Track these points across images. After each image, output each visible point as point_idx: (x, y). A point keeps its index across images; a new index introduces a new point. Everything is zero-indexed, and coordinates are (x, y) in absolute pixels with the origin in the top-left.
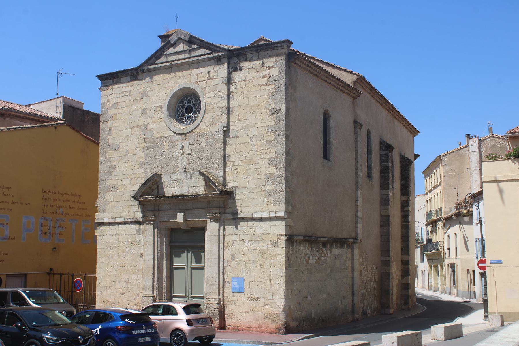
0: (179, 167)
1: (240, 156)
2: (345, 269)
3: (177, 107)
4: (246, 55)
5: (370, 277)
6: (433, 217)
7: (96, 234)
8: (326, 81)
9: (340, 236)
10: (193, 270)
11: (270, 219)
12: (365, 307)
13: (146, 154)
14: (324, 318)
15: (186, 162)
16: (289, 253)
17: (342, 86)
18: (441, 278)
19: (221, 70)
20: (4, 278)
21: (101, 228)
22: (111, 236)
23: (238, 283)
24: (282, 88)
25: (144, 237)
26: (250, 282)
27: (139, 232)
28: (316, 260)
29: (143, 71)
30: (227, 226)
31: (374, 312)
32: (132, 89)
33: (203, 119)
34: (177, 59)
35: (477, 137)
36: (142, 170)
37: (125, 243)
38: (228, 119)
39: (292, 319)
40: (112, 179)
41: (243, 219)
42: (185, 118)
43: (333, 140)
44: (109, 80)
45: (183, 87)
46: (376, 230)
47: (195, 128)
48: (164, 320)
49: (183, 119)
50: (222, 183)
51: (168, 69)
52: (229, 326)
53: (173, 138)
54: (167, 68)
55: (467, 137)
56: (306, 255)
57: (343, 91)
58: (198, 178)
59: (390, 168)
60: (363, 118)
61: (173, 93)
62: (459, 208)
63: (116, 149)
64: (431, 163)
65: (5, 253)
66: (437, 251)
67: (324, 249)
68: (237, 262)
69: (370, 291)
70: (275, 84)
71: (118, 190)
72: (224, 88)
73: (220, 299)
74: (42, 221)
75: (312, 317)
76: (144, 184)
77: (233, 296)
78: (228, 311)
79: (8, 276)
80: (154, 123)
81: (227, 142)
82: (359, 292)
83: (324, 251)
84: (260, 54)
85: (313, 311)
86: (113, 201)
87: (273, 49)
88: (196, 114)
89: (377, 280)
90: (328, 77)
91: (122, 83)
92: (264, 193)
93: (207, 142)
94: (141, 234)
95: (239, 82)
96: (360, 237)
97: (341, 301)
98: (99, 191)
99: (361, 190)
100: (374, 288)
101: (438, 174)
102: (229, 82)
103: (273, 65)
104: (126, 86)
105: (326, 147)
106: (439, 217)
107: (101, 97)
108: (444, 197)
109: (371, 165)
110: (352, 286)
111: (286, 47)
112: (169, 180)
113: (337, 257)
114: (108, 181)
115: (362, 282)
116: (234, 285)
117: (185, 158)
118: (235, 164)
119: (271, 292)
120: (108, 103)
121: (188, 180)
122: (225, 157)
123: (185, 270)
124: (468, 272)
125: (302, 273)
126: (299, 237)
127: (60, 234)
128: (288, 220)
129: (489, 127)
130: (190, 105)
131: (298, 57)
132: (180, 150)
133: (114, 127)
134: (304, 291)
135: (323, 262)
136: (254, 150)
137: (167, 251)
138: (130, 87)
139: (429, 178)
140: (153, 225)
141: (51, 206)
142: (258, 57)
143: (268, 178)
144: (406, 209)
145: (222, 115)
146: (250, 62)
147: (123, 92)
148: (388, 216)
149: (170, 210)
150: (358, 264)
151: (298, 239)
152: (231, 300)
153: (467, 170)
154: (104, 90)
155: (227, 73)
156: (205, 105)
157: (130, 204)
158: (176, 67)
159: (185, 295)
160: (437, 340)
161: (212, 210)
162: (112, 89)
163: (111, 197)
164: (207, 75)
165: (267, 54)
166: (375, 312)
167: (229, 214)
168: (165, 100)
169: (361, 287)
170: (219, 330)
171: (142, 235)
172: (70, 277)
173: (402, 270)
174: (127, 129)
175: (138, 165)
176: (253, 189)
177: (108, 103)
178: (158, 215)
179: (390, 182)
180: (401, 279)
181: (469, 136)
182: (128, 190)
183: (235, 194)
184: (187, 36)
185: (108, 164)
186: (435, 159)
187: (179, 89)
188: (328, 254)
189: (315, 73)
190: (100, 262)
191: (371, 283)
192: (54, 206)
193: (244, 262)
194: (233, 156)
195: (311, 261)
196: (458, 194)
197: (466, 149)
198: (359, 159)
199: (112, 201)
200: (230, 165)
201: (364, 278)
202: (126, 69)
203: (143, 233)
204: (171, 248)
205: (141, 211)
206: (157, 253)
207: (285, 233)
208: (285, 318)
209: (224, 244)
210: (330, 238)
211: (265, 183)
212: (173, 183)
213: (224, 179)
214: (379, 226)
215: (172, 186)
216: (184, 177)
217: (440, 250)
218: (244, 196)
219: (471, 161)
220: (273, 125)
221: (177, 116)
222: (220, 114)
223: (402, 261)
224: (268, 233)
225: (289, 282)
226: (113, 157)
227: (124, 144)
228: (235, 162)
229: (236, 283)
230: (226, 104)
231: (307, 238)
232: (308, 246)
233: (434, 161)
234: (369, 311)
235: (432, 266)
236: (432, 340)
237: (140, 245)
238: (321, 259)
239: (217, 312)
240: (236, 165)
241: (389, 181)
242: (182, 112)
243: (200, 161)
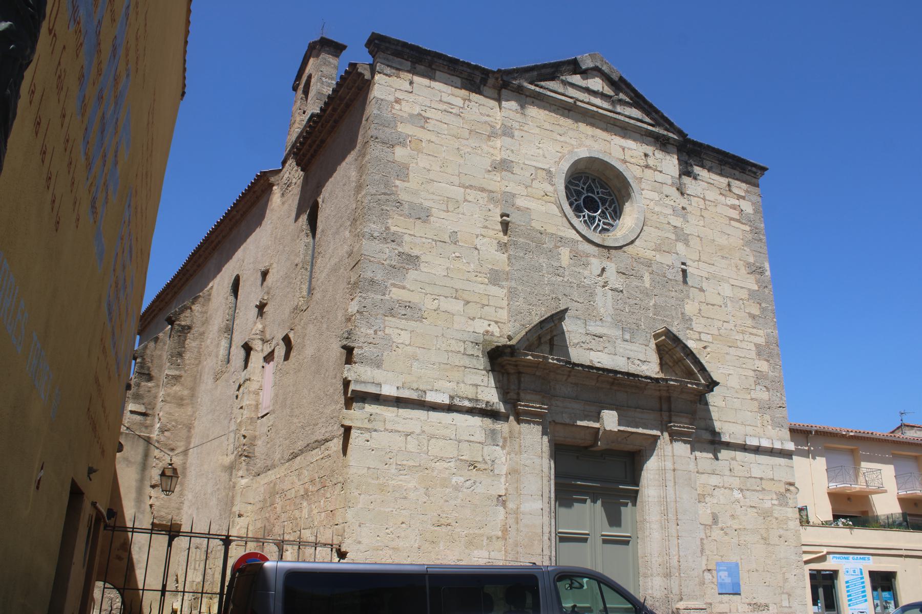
15: (613, 305)
21: (366, 409)
23: (729, 575)
25: (509, 453)
26: (748, 571)
27: (494, 440)
34: (587, 100)
37: (448, 460)
40: (408, 286)
41: (728, 446)
44: (403, 58)
45: (597, 157)
54: (559, 107)
61: (576, 158)
63: (420, 219)
70: (750, 226)
71: (424, 320)
77: (721, 602)
84: (724, 169)
86: (410, 345)
87: (743, 171)
94: (497, 445)
103: (743, 194)
104: (449, 92)
112: (583, 331)
114: (394, 290)
121: (626, 343)
130: (584, 196)
145: (676, 240)
149: (576, 398)
154: (385, 72)
157: (462, 363)
158: (579, 113)
171: (503, 447)
176: (737, 392)
177: (397, 106)
182: (456, 326)
185: (394, 247)
190: (360, 506)
193: (736, 530)
194: (698, 321)
199: (407, 343)
205: (496, 388)
212: (593, 341)
215: (591, 347)
216: (617, 334)
222: (673, 237)
224: (769, 477)
227: (443, 215)
229: (726, 573)
237: (496, 472)
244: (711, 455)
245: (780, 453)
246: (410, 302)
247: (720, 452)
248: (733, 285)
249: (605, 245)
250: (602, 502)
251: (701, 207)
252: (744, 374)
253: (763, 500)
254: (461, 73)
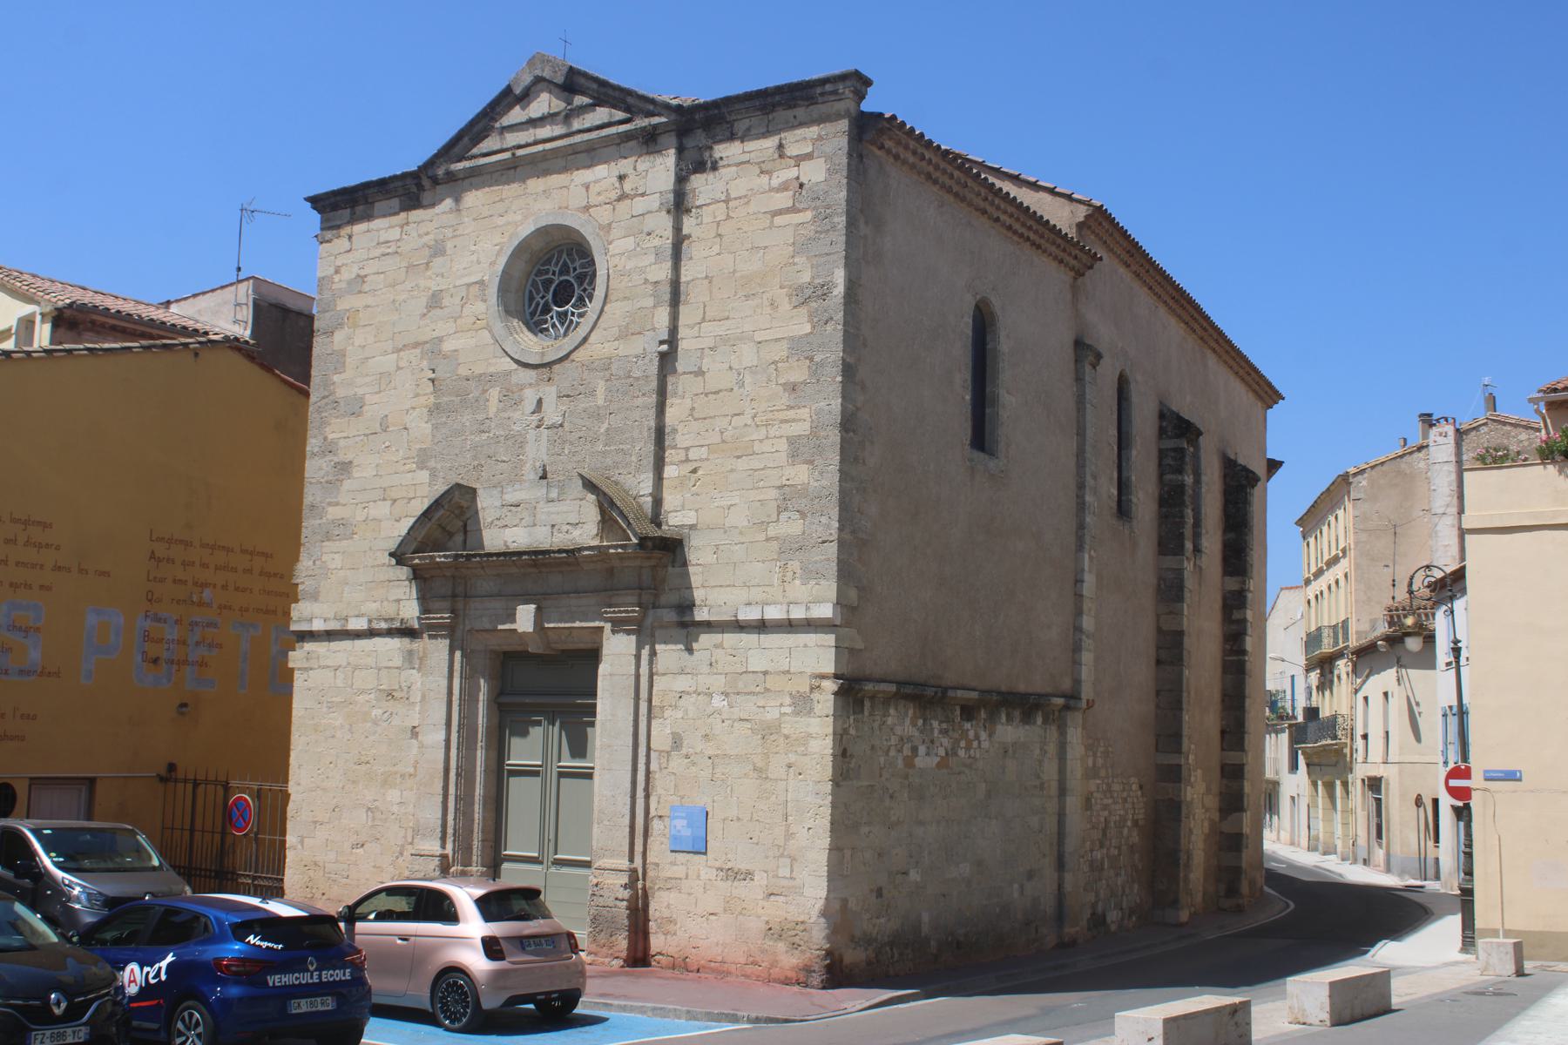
0: (528, 466)
1: (707, 430)
2: (1035, 787)
3: (529, 287)
4: (731, 124)
5: (1118, 812)
6: (1323, 647)
7: (291, 665)
8: (984, 212)
9: (1022, 688)
10: (561, 779)
11: (790, 626)
12: (1100, 904)
13: (435, 427)
16: (848, 734)
17: (1036, 232)
18: (1342, 818)
19: (655, 169)
20: (21, 790)
21: (305, 649)
22: (333, 673)
23: (689, 825)
24: (836, 220)
27: (411, 662)
28: (938, 759)
29: (435, 181)
30: (660, 643)
31: (1130, 916)
32: (403, 234)
33: (601, 320)
34: (531, 140)
35: (1451, 421)
36: (424, 476)
38: (674, 317)
39: (852, 941)
40: (342, 501)
41: (709, 626)
42: (552, 318)
43: (1006, 395)
46: (1141, 672)
47: (576, 348)
48: (416, 936)
49: (546, 322)
50: (650, 514)
51: (504, 172)
52: (661, 957)
53: (514, 379)
54: (503, 170)
55: (1423, 421)
56: (905, 741)
57: (1039, 247)
58: (581, 500)
59: (1189, 491)
60: (1104, 335)
61: (517, 243)
62: (1396, 620)
64: (1322, 494)
65: (29, 715)
66: (1334, 742)
67: (967, 725)
68: (687, 757)
69: (1119, 855)
70: (815, 208)
71: (355, 536)
72: (664, 223)
73: (634, 871)
74: (148, 624)
75: (923, 934)
76: (422, 518)
77: (673, 864)
78: (656, 908)
79: (34, 781)
80: (461, 334)
81: (669, 387)
82: (1083, 857)
83: (968, 730)
84: (774, 119)
85: (926, 918)
87: (811, 100)
88: (585, 306)
89: (1140, 823)
90: (990, 198)
91: (378, 217)
92: (775, 545)
93: (609, 390)
94: (414, 668)
95: (709, 204)
96: (1087, 692)
97: (1022, 887)
98: (303, 537)
99: (1095, 551)
100: (1132, 847)
101: (1341, 527)
102: (680, 205)
103: (809, 149)
105: (983, 414)
106: (1341, 645)
107: (319, 261)
108: (1356, 590)
109: (1129, 478)
110: (1059, 838)
111: (851, 95)
112: (498, 503)
113: (1010, 751)
114: (330, 509)
115: (1093, 828)
116: (678, 828)
117: (544, 438)
118: (691, 456)
119: (785, 854)
120: (337, 278)
122: (660, 434)
123: (539, 779)
124: (1419, 802)
125: (891, 797)
126: (882, 684)
127: (203, 664)
128: (847, 629)
129: (1487, 394)
131: (888, 126)
132: (533, 413)
133: (350, 348)
134: (897, 854)
136: (749, 412)
137: (487, 723)
138: (398, 230)
139: (1316, 538)
140: (447, 642)
141: (175, 581)
142: (768, 126)
143: (788, 498)
144: (1236, 615)
146: (742, 142)
147: (378, 244)
148: (1181, 633)
150: (1079, 773)
151: (879, 692)
152: (669, 874)
153: (1421, 513)
154: (326, 239)
155: (672, 179)
156: (608, 276)
159: (536, 855)
160: (1304, 1024)
161: (617, 595)
162: (350, 237)
163: (336, 556)
164: (617, 185)
165: (795, 117)
166: (1134, 919)
167: (668, 610)
168: (493, 264)
169: (1088, 843)
170: (628, 966)
171: (419, 670)
172: (220, 790)
173: (1221, 793)
174: (385, 353)
175: (413, 460)
176: (741, 533)
177: (337, 278)
178: (464, 610)
179: (1188, 531)
180: (1217, 819)
181: (1428, 421)
183: (686, 550)
184: (560, 70)
186: (1333, 483)
187: (533, 229)
188: (979, 743)
189: (948, 182)
191: (1121, 833)
192: (186, 581)
193: (710, 758)
194: (685, 431)
196: (1394, 581)
197: (1421, 455)
198: (1088, 455)
199: (339, 567)
200: (676, 459)
201: (1099, 815)
202: (387, 176)
203: (421, 664)
204: (501, 711)
205: (418, 599)
206: (459, 726)
207: (833, 671)
208: (828, 938)
209: (650, 701)
210: (989, 692)
211: (778, 516)
212: (508, 514)
213: (658, 502)
214: (1153, 662)
216: (539, 494)
217: (1340, 739)
218: (715, 553)
219: (1433, 488)
220: (806, 334)
221: (528, 311)
222: (650, 302)
223: (1223, 767)
225: (843, 826)
226: (345, 438)
227: (376, 398)
228: (691, 450)
230: (670, 271)
231: (909, 690)
232: (915, 713)
233: (1328, 489)
234: (1113, 916)
235: (1320, 783)
236: (1290, 1023)
237: (412, 700)
238: (956, 754)
239: (622, 910)
240: (695, 458)
241: (1183, 527)
242: (542, 302)
243: (587, 447)
244: (681, 647)
245: (809, 625)
246: (343, 519)
247: (697, 641)
248: (760, 343)
249: (545, 362)
250: (561, 723)
251: (718, 219)
252: (758, 498)
253: (764, 707)
254: (396, 191)
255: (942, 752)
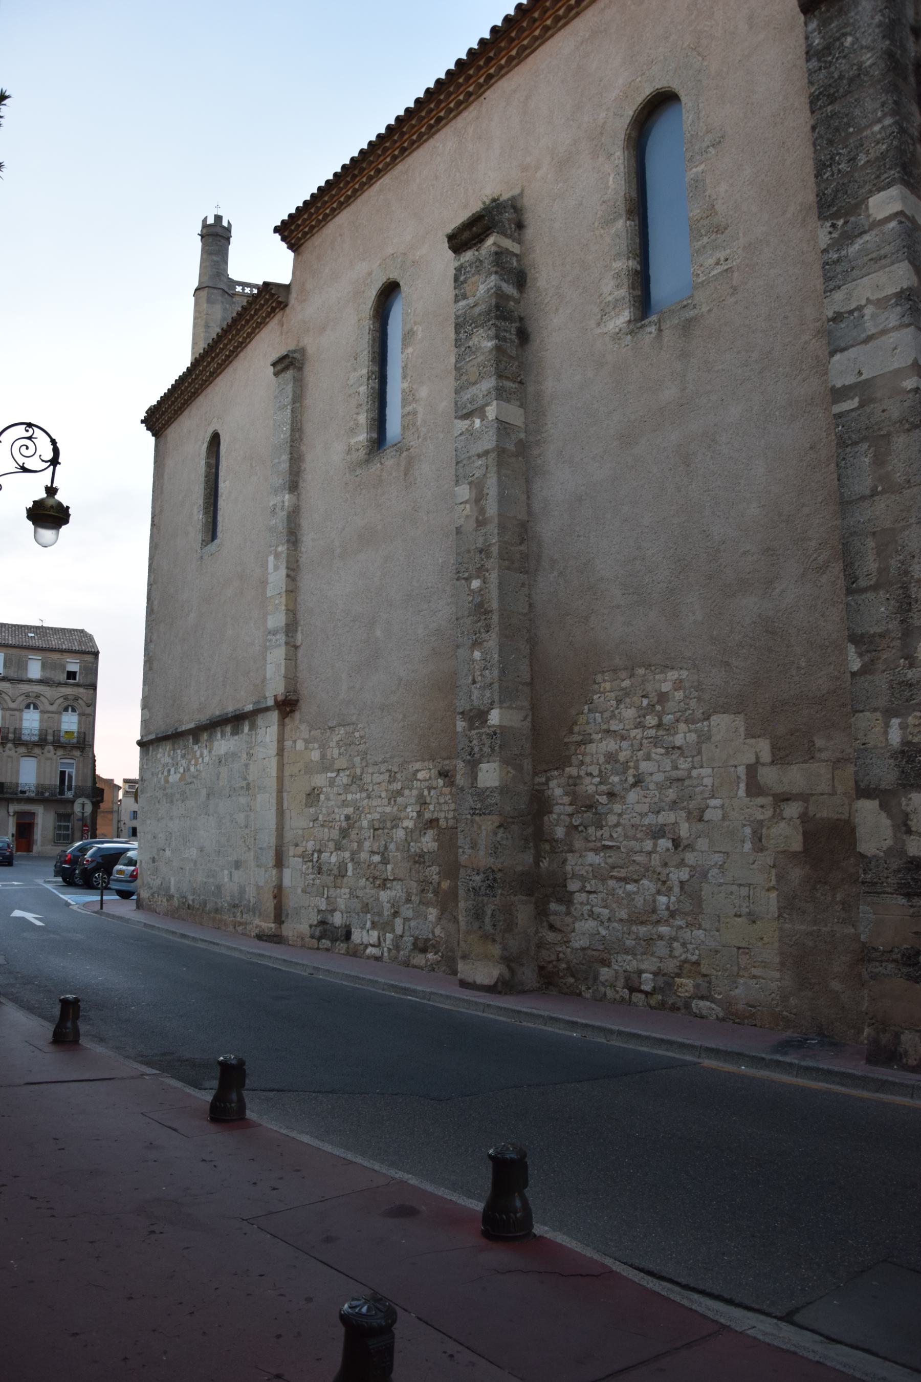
2: (242, 788)
14: (191, 903)
67: (196, 747)
85: (173, 882)
97: (231, 874)
113: (223, 761)
135: (194, 777)
195: (171, 779)
238: (189, 770)
255: (181, 770)
